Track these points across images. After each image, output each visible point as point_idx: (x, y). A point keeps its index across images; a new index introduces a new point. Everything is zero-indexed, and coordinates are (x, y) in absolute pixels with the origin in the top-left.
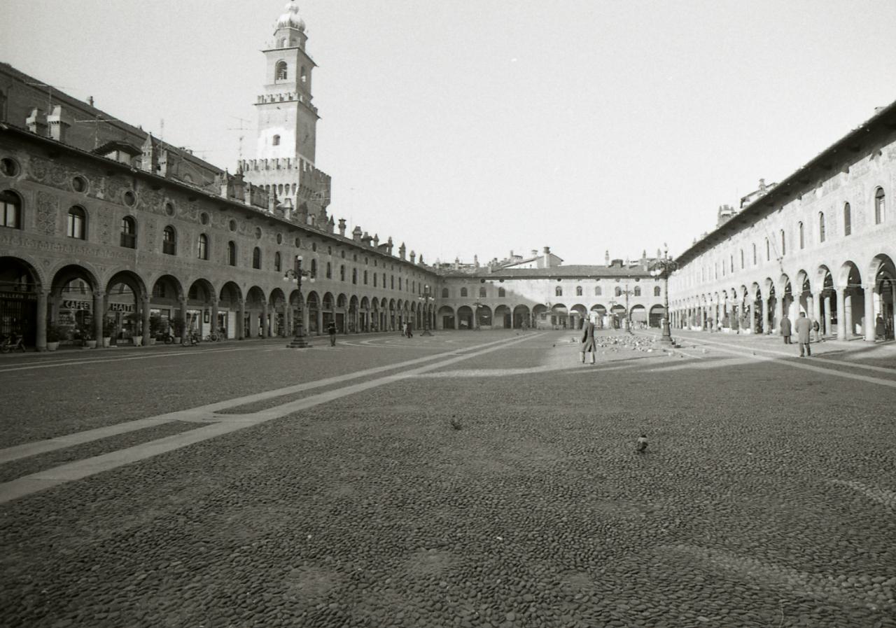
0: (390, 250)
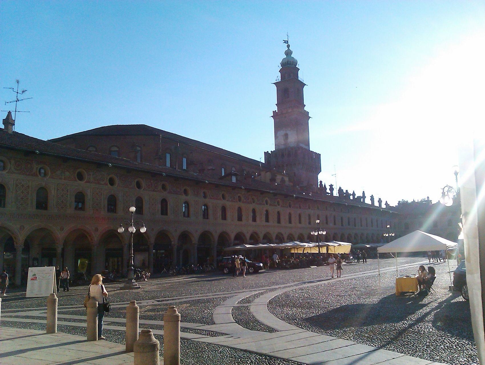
0: (364, 200)
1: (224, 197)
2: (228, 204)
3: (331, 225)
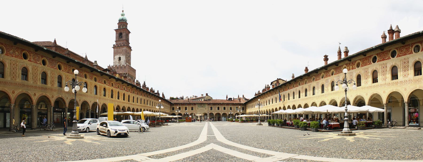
1: (105, 83)
2: (107, 87)
3: (149, 105)
